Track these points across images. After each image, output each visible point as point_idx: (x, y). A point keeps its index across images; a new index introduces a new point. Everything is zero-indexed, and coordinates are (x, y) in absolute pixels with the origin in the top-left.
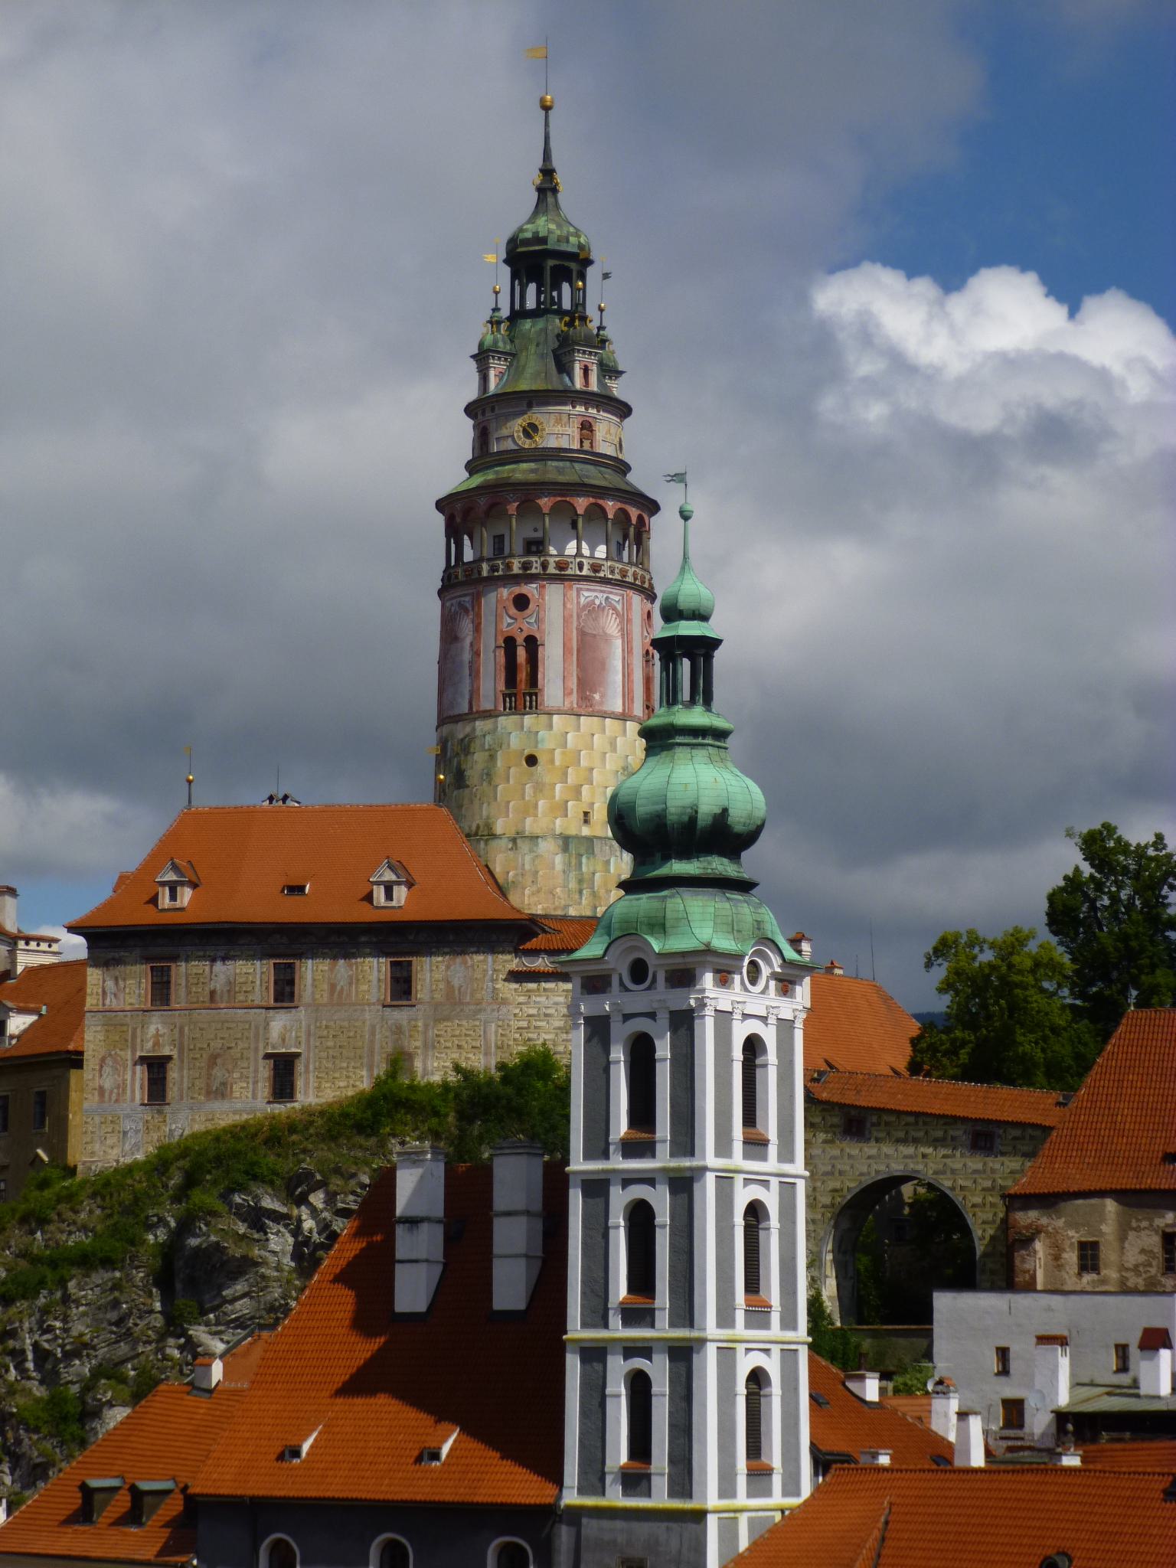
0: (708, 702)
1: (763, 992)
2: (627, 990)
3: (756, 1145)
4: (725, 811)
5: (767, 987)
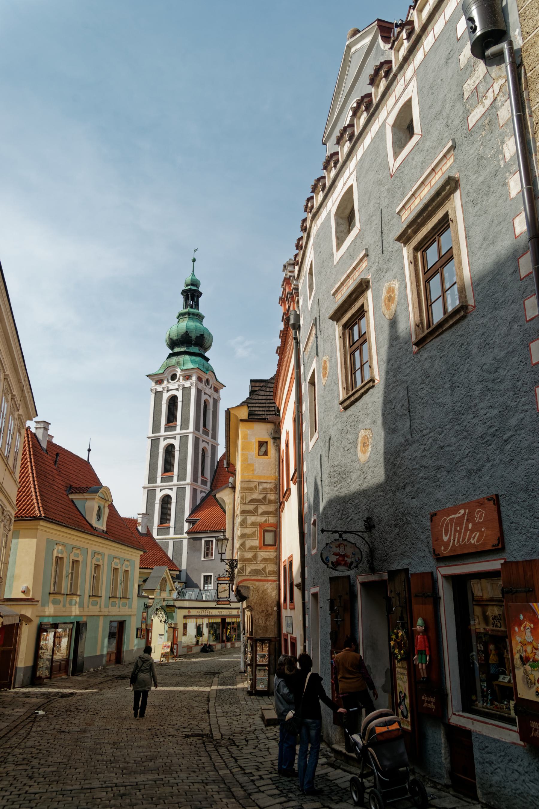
0: (198, 309)
1: (211, 388)
2: (169, 383)
3: (206, 433)
4: (202, 335)
5: (211, 387)
